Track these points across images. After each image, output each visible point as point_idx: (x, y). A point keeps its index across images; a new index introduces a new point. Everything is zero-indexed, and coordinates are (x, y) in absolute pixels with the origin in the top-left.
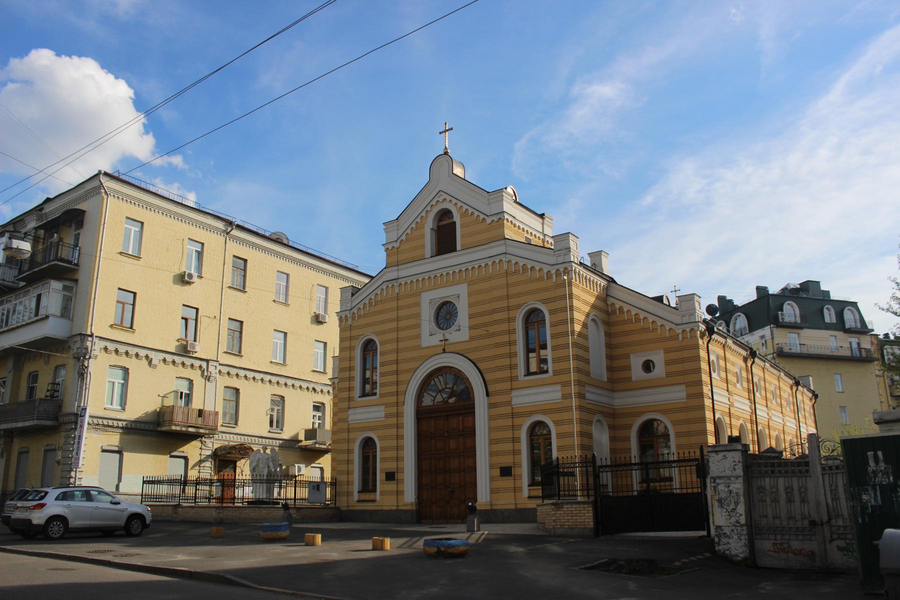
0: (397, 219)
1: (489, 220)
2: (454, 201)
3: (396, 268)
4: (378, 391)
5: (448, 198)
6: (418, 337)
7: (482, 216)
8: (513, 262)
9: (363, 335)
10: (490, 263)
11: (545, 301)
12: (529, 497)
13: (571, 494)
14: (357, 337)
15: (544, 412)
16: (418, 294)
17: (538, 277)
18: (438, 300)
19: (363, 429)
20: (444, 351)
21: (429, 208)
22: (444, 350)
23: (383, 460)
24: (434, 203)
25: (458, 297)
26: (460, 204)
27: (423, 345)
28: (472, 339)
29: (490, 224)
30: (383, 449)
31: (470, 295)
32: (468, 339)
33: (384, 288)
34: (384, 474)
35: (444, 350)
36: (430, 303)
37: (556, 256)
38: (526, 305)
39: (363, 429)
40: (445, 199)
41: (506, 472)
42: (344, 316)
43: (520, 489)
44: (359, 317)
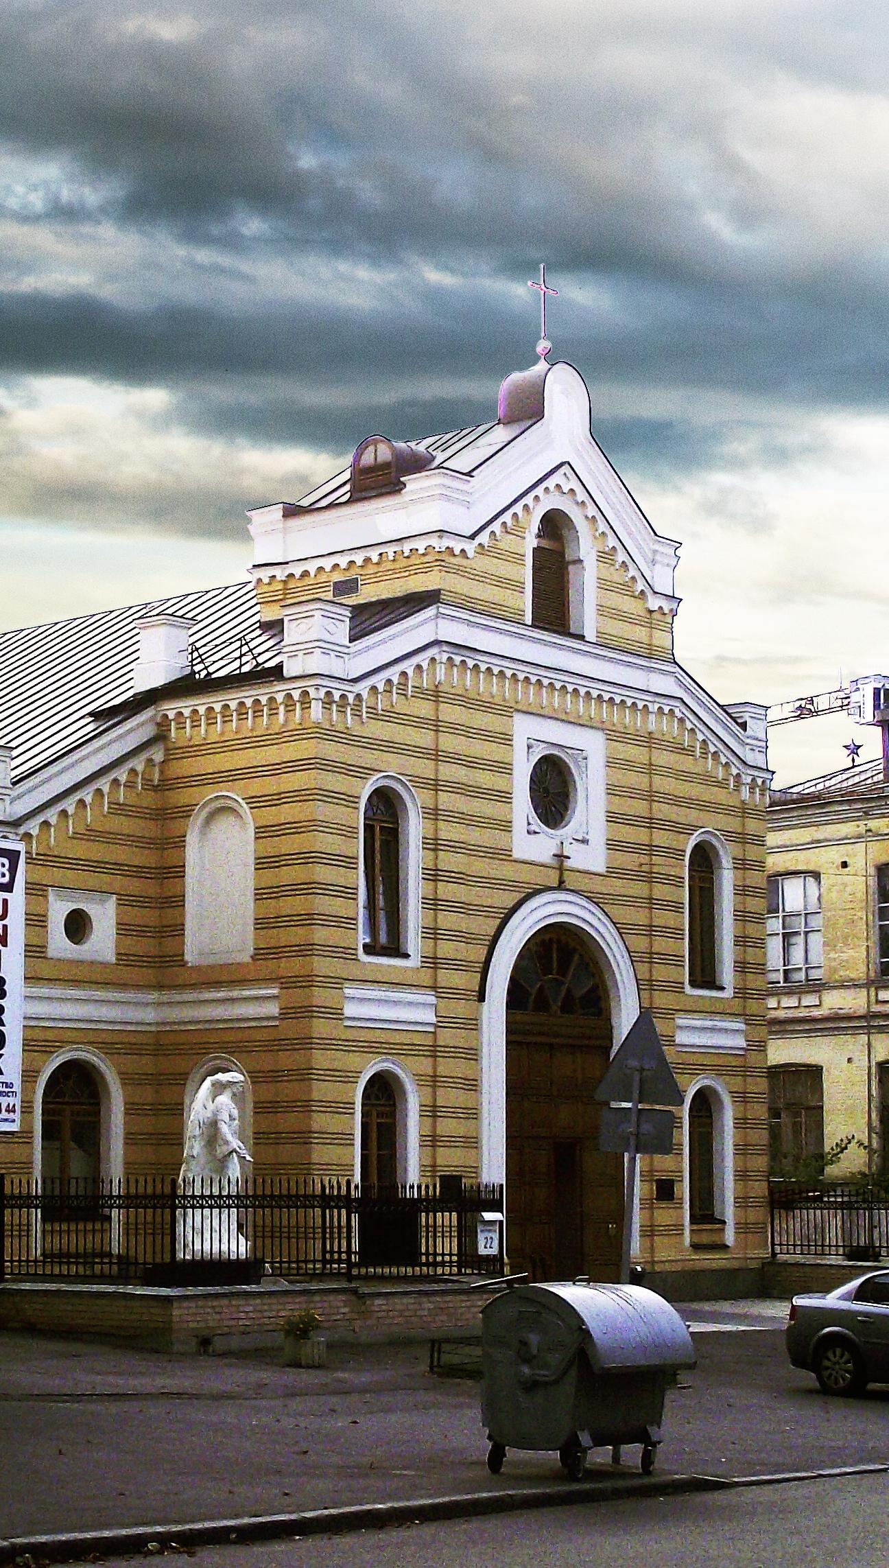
0: (469, 474)
1: (654, 603)
2: (591, 511)
3: (465, 615)
4: (414, 941)
5: (581, 496)
6: (506, 826)
7: (641, 585)
8: (689, 726)
9: (381, 771)
10: (653, 708)
11: (729, 835)
12: (696, 1247)
13: (151, 1231)
14: (364, 772)
15: (720, 1070)
16: (507, 710)
17: (720, 779)
18: (546, 745)
19: (373, 1048)
20: (561, 886)
21: (539, 491)
22: (561, 882)
23: (432, 1141)
24: (551, 483)
25: (586, 759)
26: (602, 527)
27: (516, 854)
28: (613, 872)
29: (651, 612)
30: (432, 1112)
31: (611, 763)
32: (601, 869)
33: (445, 656)
34: (438, 1180)
35: (561, 882)
36: (529, 747)
37: (748, 747)
38: (703, 830)
39: (373, 1048)
40: (572, 490)
41: (665, 1190)
42: (337, 695)
43: (679, 1227)
44: (374, 714)
